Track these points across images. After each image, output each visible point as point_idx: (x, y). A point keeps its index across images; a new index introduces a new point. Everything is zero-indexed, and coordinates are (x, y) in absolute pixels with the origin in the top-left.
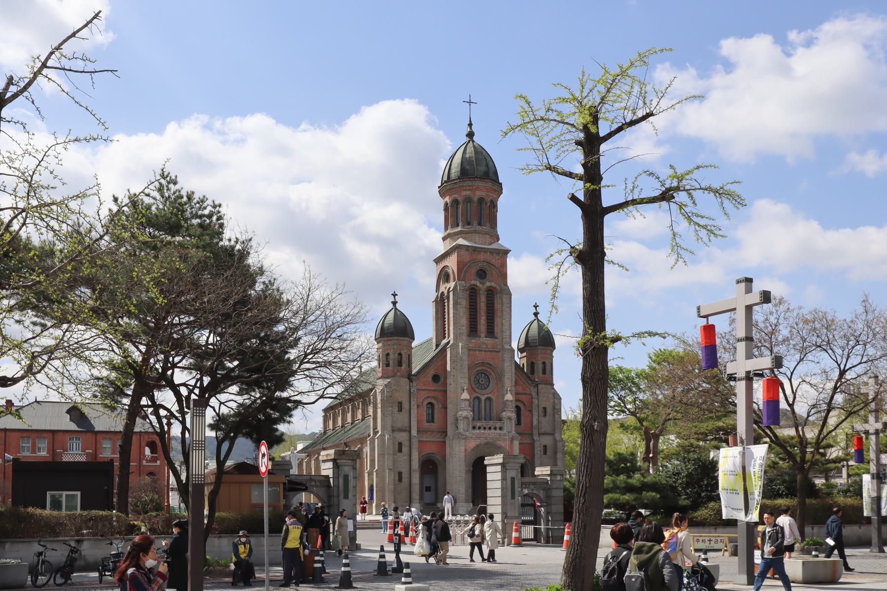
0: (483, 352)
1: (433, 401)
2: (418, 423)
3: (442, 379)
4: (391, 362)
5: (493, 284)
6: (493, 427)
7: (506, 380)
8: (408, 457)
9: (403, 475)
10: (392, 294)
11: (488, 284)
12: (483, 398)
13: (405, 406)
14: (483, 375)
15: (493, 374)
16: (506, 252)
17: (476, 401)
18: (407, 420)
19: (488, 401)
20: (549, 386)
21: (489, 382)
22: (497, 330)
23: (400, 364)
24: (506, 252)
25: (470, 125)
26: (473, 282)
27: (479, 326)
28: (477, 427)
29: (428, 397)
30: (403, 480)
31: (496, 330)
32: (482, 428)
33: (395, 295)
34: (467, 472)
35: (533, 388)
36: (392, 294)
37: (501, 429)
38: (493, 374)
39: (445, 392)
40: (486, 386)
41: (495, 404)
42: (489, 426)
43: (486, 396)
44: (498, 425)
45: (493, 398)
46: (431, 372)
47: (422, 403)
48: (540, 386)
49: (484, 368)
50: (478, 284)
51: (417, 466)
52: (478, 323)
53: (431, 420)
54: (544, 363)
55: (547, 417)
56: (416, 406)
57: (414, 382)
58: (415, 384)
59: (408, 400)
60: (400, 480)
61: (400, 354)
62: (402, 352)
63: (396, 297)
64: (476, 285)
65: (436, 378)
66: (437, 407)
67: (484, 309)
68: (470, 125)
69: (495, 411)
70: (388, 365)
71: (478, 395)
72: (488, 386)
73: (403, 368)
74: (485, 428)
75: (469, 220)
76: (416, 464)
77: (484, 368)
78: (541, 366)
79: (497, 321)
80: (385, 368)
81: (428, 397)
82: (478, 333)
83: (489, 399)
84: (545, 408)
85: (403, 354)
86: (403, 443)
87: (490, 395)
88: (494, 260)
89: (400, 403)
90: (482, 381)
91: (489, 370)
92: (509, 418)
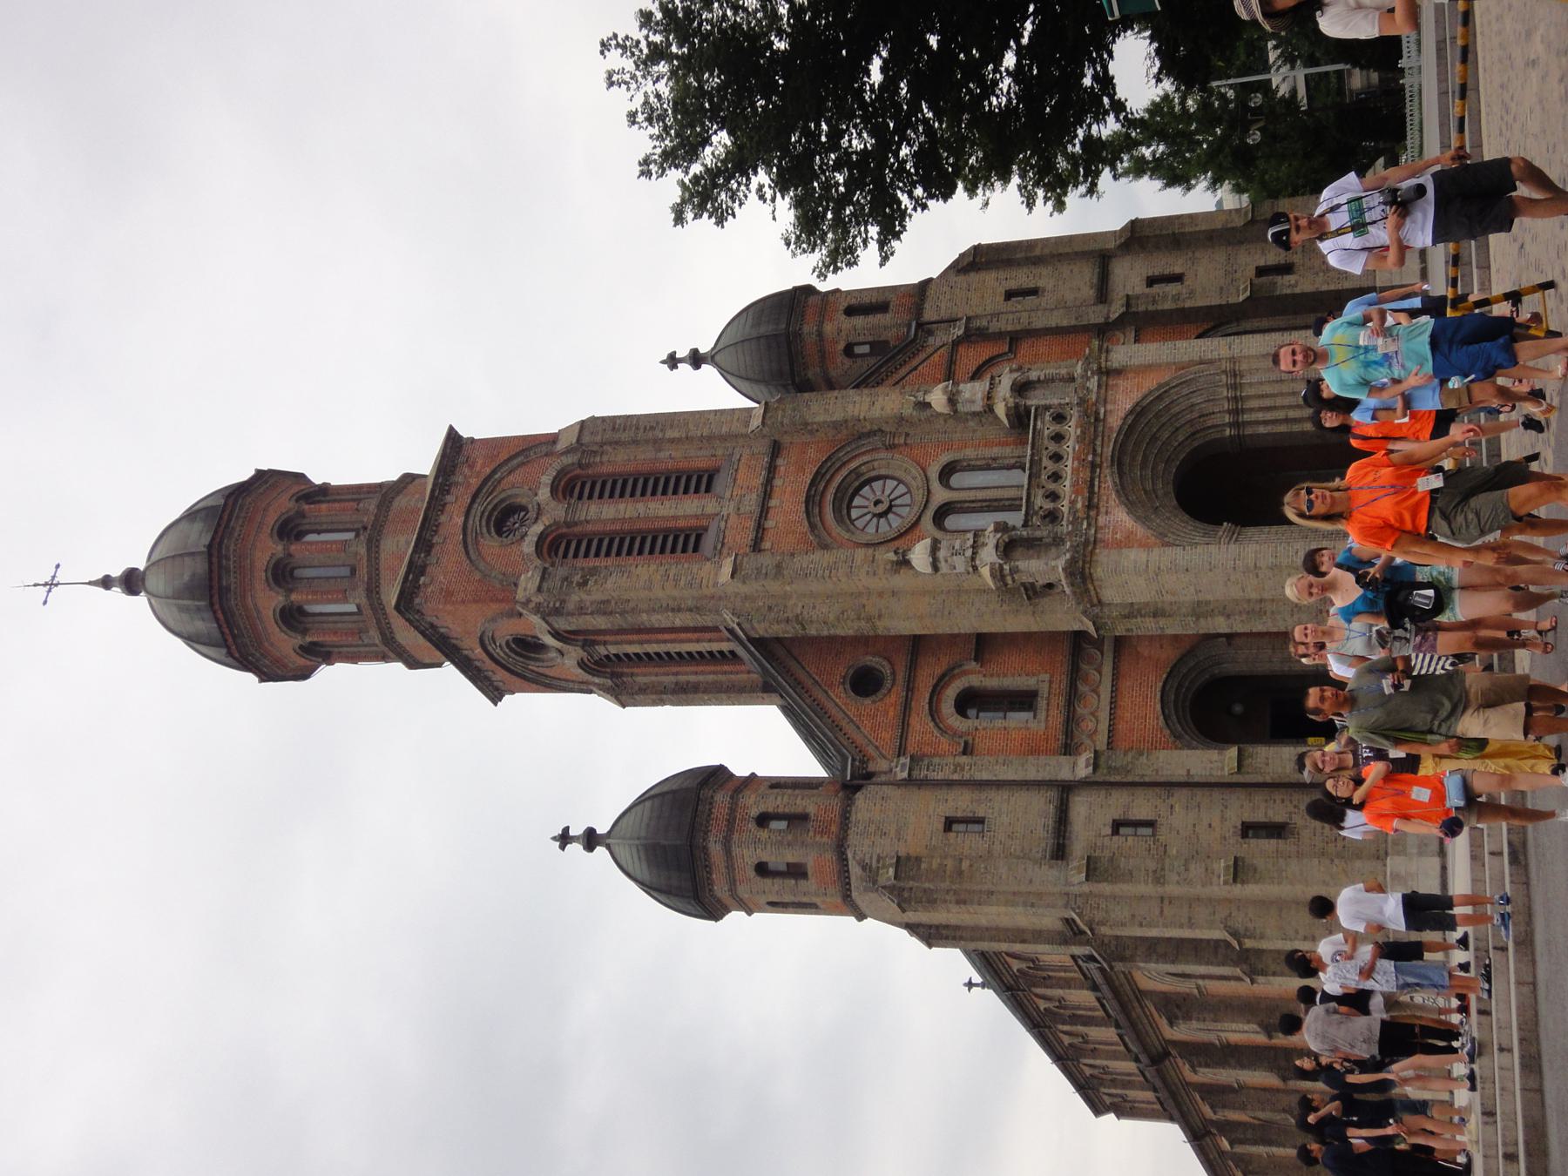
0: (773, 503)
1: (951, 693)
2: (1034, 751)
3: (871, 660)
4: (791, 856)
5: (547, 479)
6: (1053, 447)
7: (876, 412)
8: (1181, 795)
9: (1259, 817)
10: (563, 847)
11: (544, 494)
12: (940, 495)
13: (961, 803)
14: (857, 501)
15: (853, 465)
16: (454, 441)
17: (952, 522)
18: (1021, 798)
19: (956, 480)
20: (931, 292)
21: (885, 477)
22: (700, 459)
23: (797, 820)
24: (454, 441)
25: (106, 583)
26: (528, 546)
27: (681, 523)
28: (1049, 505)
29: (934, 712)
30: (1279, 817)
31: (702, 464)
32: (1051, 486)
33: (564, 839)
34: (1233, 537)
35: (931, 340)
36: (563, 847)
37: (1060, 418)
38: (853, 465)
39: (917, 645)
40: (902, 489)
41: (970, 453)
42: (1046, 462)
43: (935, 485)
44: (1048, 427)
45: (945, 458)
46: (841, 700)
47: (955, 734)
48: (929, 314)
49: (829, 497)
50: (538, 529)
51: (1213, 755)
52: (671, 524)
53: (1024, 700)
54: (851, 311)
55: (1041, 284)
56: (964, 759)
57: (871, 767)
58: (882, 765)
59: (942, 793)
60: (1276, 830)
61: (763, 820)
62: (754, 812)
63: (572, 833)
64: (542, 537)
65: (865, 683)
66: (975, 678)
67: (622, 506)
68: (106, 583)
69: (996, 451)
70: (796, 872)
71: (930, 513)
72: (900, 481)
73: (811, 810)
74: (1056, 477)
75: (345, 571)
76: (1218, 761)
77: (829, 497)
78: (859, 321)
79: (671, 458)
80: (810, 885)
81: (934, 712)
82: (704, 523)
83: (947, 473)
84: (1009, 295)
85: (762, 808)
86: (1117, 814)
87: (934, 471)
88: (468, 479)
89: (949, 824)
90: (877, 503)
91: (838, 479)
92: (1021, 388)
